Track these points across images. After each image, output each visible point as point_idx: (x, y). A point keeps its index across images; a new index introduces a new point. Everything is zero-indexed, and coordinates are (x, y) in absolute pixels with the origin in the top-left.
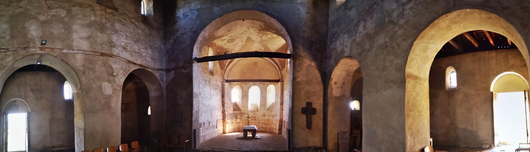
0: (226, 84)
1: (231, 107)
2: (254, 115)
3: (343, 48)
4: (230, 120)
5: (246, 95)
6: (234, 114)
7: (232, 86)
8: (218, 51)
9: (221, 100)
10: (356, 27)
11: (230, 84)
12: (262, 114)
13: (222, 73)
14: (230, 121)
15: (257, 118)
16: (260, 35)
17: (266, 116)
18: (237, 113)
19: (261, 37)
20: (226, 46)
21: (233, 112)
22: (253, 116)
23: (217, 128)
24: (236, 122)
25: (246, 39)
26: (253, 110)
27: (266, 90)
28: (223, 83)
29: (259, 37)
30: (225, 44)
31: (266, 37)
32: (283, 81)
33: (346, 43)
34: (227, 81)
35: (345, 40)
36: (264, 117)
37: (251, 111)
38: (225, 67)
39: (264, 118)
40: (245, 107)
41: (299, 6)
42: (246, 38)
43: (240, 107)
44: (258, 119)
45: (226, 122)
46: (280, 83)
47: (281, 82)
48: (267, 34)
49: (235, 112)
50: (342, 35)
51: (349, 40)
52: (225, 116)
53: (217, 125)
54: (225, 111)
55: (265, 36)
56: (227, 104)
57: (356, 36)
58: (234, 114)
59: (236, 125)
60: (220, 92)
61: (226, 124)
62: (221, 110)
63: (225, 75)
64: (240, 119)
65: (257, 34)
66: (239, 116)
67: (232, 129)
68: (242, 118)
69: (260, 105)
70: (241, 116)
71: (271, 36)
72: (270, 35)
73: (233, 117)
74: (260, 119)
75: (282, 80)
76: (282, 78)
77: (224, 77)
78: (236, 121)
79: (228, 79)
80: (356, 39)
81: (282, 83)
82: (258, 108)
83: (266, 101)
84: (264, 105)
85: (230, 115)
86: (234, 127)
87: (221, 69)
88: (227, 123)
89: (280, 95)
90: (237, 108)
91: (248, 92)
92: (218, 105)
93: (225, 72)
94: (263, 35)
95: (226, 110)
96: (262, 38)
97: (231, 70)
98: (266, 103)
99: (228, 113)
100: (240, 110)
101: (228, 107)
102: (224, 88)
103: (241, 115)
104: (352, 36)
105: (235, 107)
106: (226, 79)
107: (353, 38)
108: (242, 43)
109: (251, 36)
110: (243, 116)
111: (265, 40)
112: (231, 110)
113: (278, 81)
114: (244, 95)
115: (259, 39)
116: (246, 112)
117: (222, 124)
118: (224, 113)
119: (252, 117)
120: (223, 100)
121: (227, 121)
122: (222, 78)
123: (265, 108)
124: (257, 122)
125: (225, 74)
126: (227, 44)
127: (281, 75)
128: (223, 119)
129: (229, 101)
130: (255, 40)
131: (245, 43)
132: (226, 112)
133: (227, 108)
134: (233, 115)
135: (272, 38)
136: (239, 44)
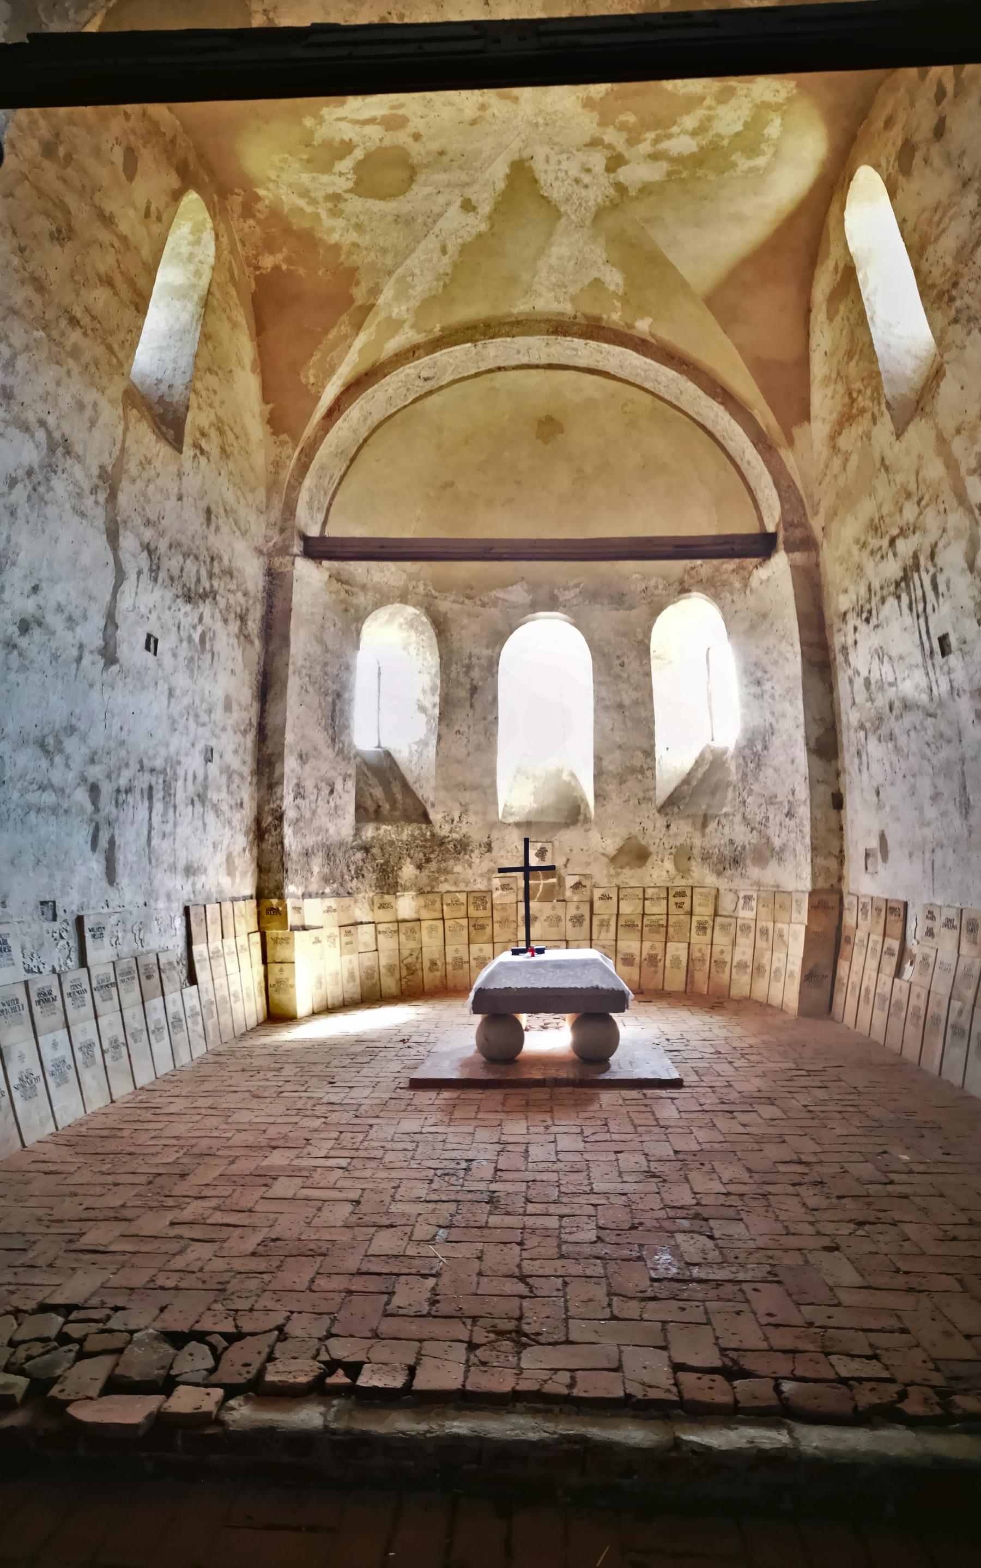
1: (339, 786)
4: (331, 902)
6: (366, 849)
12: (611, 845)
13: (277, 465)
14: (329, 910)
18: (392, 843)
23: (192, 979)
24: (381, 915)
26: (541, 811)
28: (277, 561)
36: (627, 872)
37: (518, 825)
38: (309, 415)
39: (630, 877)
40: (462, 787)
43: (426, 791)
44: (577, 886)
45: (292, 919)
49: (369, 832)
52: (283, 868)
53: (199, 949)
54: (279, 817)
56: (303, 758)
59: (387, 944)
61: (287, 941)
62: (249, 812)
63: (304, 496)
64: (421, 892)
66: (408, 871)
67: (352, 976)
68: (434, 880)
70: (433, 866)
73: (359, 874)
74: (597, 893)
77: (290, 509)
78: (383, 906)
79: (331, 532)
82: (583, 800)
85: (330, 856)
86: (368, 960)
88: (304, 928)
90: (392, 801)
92: (209, 756)
93: (303, 468)
95: (290, 814)
99: (310, 841)
101: (309, 784)
102: (288, 613)
103: (428, 860)
105: (378, 792)
106: (314, 532)
110: (446, 871)
112: (336, 812)
116: (472, 828)
117: (256, 937)
118: (270, 839)
121: (298, 909)
122: (276, 514)
125: (308, 482)
128: (260, 895)
129: (319, 737)
132: (288, 831)
133: (299, 794)
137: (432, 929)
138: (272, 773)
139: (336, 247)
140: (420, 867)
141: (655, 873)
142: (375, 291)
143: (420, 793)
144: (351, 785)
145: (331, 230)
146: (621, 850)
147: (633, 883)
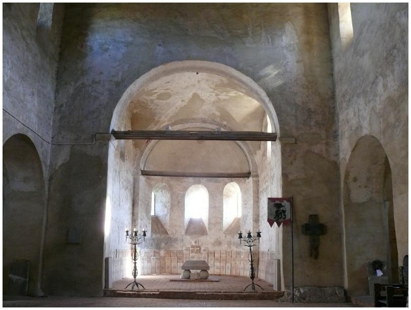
0: (142, 179)
2: (195, 242)
3: (360, 122)
5: (179, 202)
6: (153, 240)
7: (153, 183)
8: (135, 111)
9: (131, 211)
10: (374, 85)
11: (147, 178)
12: (213, 241)
15: (203, 249)
16: (216, 92)
17: (223, 244)
19: (217, 95)
20: (152, 104)
21: (152, 236)
22: (193, 244)
25: (191, 97)
27: (221, 193)
29: (214, 94)
30: (153, 100)
31: (227, 96)
32: (257, 176)
33: (363, 113)
34: (144, 173)
35: (361, 107)
36: (217, 247)
41: (285, 51)
42: (190, 95)
44: (204, 250)
46: (251, 179)
47: (253, 177)
48: (228, 92)
50: (355, 98)
51: (367, 108)
55: (225, 93)
56: (141, 219)
57: (376, 101)
58: (153, 240)
60: (131, 194)
65: (212, 90)
66: (163, 245)
69: (209, 223)
70: (169, 244)
71: (234, 93)
72: (234, 92)
75: (255, 174)
76: (254, 170)
80: (376, 106)
81: (254, 179)
83: (222, 214)
84: (217, 223)
87: (136, 148)
89: (251, 202)
91: (183, 196)
94: (221, 92)
96: (219, 97)
97: (152, 150)
98: (222, 219)
100: (167, 233)
101: (142, 225)
102: (138, 188)
104: (369, 102)
107: (371, 105)
108: (184, 103)
109: (199, 92)
111: (225, 100)
113: (247, 175)
114: (176, 203)
115: (213, 98)
119: (192, 247)
120: (135, 211)
123: (221, 229)
124: (203, 256)
126: (157, 101)
127: (252, 162)
130: (206, 99)
131: (186, 104)
134: (152, 241)
135: (235, 97)
136: (176, 104)
137: (168, 259)
138: (135, 223)
139: (151, 109)
140: (165, 244)
141: (223, 247)
142: (160, 118)
143: (165, 227)
144: (150, 225)
145: (150, 106)
146: (215, 242)
147: (218, 249)
